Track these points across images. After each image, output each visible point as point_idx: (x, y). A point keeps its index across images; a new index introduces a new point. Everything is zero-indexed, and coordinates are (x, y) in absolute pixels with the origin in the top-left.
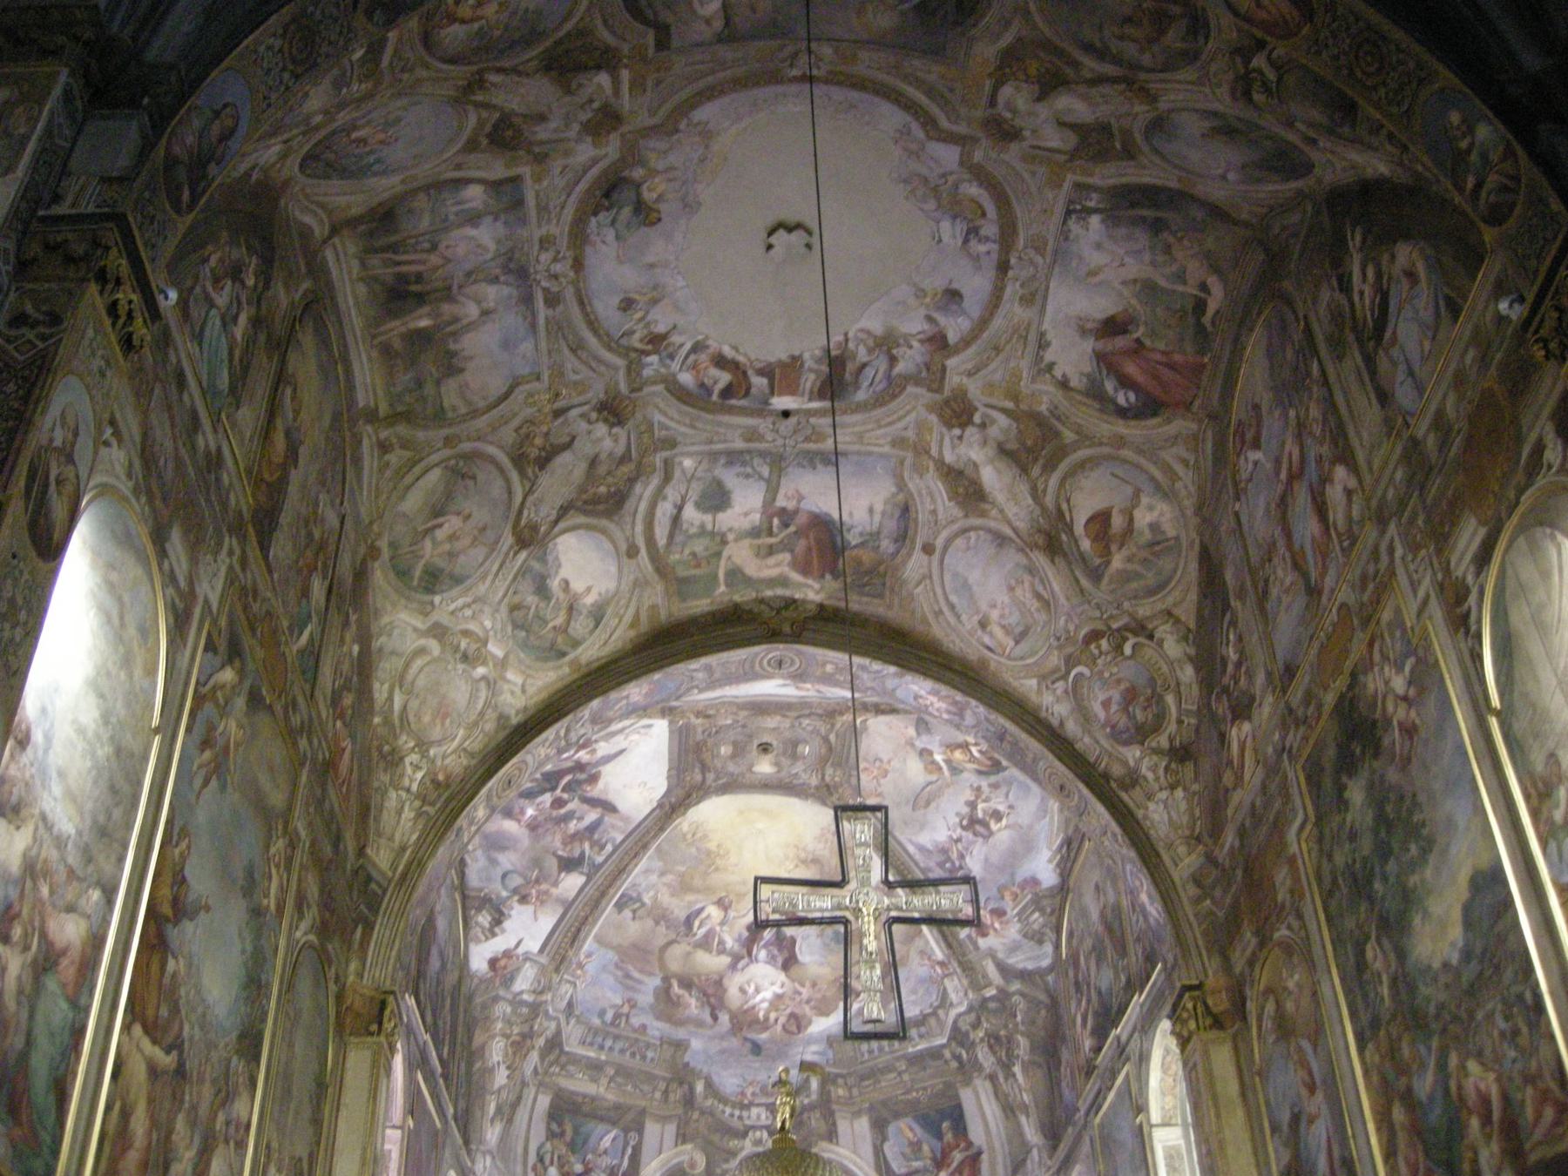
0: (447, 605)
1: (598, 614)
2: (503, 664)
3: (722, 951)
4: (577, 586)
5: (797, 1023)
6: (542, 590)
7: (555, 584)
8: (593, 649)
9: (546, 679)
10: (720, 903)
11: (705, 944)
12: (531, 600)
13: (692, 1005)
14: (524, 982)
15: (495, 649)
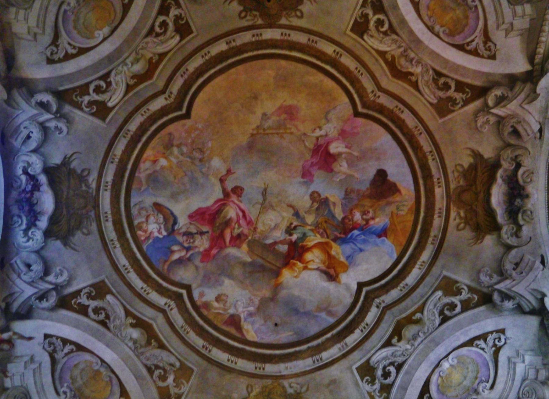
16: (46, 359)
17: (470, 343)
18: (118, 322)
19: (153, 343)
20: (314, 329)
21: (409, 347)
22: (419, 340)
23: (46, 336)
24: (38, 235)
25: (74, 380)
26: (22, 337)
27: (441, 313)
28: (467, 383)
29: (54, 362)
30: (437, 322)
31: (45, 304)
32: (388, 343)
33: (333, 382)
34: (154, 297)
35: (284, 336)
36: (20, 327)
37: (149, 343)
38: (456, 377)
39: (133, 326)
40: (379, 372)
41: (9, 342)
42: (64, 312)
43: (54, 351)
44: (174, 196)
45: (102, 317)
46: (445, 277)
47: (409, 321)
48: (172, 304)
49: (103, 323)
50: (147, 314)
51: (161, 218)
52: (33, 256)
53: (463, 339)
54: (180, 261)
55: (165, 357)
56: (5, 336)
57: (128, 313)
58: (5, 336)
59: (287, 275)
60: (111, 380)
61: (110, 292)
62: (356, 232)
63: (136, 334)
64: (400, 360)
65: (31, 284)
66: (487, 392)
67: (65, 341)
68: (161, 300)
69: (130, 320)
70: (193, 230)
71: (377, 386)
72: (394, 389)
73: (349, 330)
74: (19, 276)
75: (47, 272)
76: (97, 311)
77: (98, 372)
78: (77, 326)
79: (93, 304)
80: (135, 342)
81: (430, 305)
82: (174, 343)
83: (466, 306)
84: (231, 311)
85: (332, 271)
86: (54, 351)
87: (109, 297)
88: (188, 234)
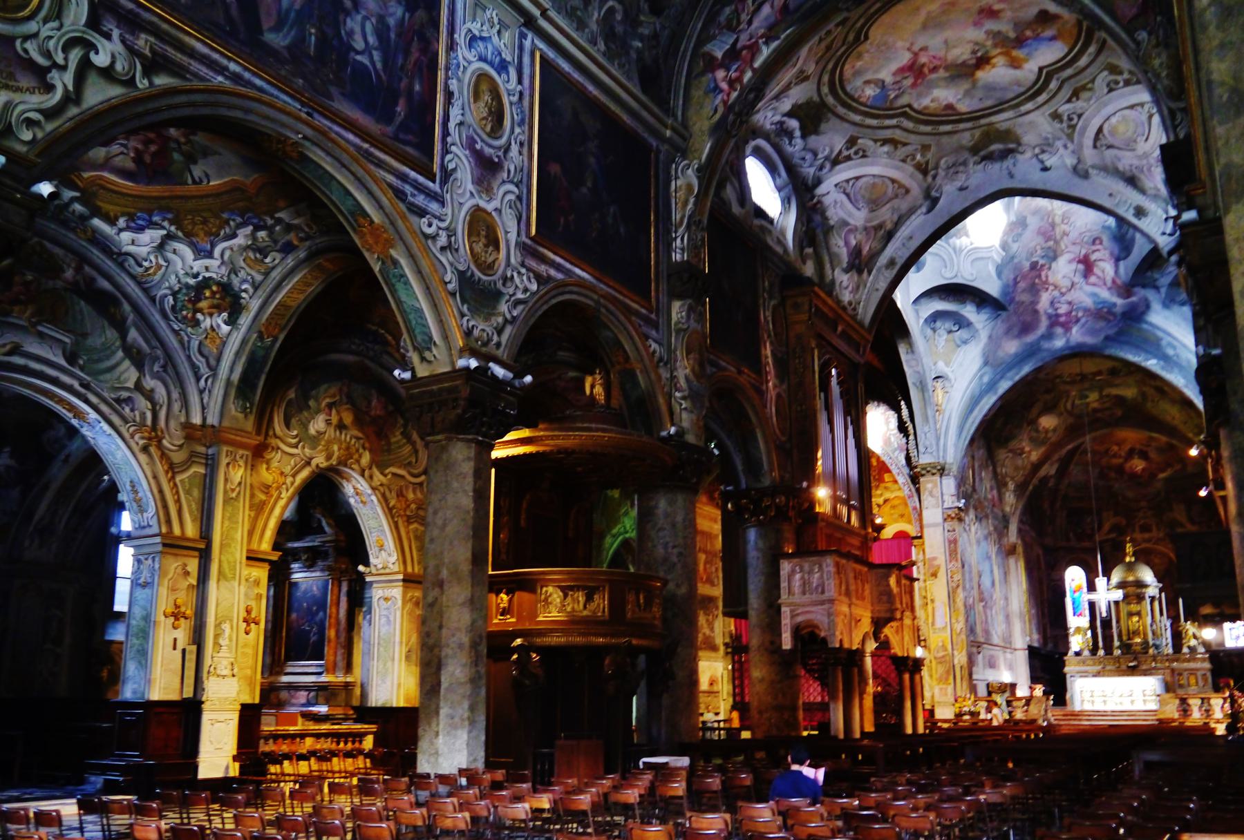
0: (1014, 444)
1: (1055, 430)
2: (1030, 452)
3: (1120, 457)
4: (1047, 426)
5: (1153, 476)
6: (1037, 431)
7: (1041, 428)
8: (1054, 438)
9: (1042, 450)
10: (1118, 444)
11: (1115, 456)
12: (1034, 434)
13: (1113, 475)
14: (1051, 484)
15: (1027, 449)
16: (844, 198)
17: (1132, 107)
18: (872, 150)
19: (899, 146)
20: (1011, 95)
21: (1085, 104)
22: (1092, 102)
23: (836, 185)
24: (798, 142)
25: (863, 197)
26: (824, 195)
27: (1108, 85)
28: (1129, 134)
29: (848, 195)
30: (1106, 90)
31: (825, 171)
32: (1069, 101)
33: (1030, 123)
34: (888, 122)
35: (989, 103)
36: (820, 190)
37: (896, 148)
38: (1121, 129)
39: (882, 145)
40: (1065, 118)
41: (819, 202)
42: (838, 168)
43: (844, 190)
44: (877, 71)
45: (861, 153)
46: (1108, 64)
47: (1084, 88)
48: (902, 119)
49: (864, 156)
50: (888, 134)
51: (872, 85)
52: (803, 153)
53: (1126, 104)
54: (897, 97)
55: (909, 149)
56: (815, 200)
57: (876, 141)
58: (815, 200)
59: (980, 74)
60: (884, 182)
61: (858, 138)
62: (1029, 42)
63: (886, 148)
64: (1079, 111)
65: (811, 166)
66: (1142, 143)
67: (847, 181)
68: (894, 122)
69: (879, 144)
70: (898, 78)
71: (1065, 125)
72: (1078, 127)
73: (1038, 93)
74: (801, 167)
75: (815, 154)
76: (856, 153)
77: (874, 185)
78: (850, 168)
79: (852, 151)
80: (887, 153)
81: (1099, 81)
82: (912, 138)
83: (1127, 83)
84: (944, 103)
85: (1015, 64)
86: (844, 190)
87: (860, 141)
88: (895, 83)
